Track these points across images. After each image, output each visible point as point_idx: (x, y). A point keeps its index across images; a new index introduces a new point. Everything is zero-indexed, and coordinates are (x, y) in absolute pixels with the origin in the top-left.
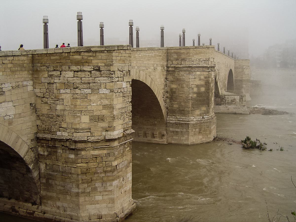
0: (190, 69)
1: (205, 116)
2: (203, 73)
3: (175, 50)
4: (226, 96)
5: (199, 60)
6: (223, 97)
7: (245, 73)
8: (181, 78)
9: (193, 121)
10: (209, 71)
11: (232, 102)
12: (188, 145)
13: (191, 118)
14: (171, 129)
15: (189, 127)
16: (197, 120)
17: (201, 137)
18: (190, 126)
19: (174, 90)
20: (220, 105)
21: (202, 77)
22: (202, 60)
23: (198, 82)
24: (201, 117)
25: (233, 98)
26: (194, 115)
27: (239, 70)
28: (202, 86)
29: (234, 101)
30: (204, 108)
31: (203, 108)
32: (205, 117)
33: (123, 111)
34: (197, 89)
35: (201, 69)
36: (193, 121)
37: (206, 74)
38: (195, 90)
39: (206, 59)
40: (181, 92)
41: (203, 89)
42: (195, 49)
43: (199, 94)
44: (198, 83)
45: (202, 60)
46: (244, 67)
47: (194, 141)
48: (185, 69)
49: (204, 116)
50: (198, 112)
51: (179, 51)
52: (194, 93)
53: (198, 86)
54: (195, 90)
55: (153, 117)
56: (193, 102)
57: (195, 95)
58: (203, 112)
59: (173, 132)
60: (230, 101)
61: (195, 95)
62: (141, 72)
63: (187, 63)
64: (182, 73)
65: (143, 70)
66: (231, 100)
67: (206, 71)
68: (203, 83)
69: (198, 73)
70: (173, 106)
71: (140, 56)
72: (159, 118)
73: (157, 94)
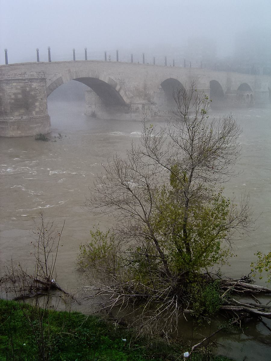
0: (8, 81)
9: (12, 120)
10: (26, 82)
12: (7, 137)
13: (11, 117)
15: (8, 124)
17: (19, 132)
18: (8, 123)
20: (128, 113)
21: (19, 87)
23: (14, 91)
28: (19, 93)
30: (22, 111)
32: (24, 117)
35: (17, 81)
36: (12, 120)
37: (22, 84)
38: (13, 97)
45: (17, 74)
47: (14, 134)
50: (17, 114)
52: (12, 99)
53: (14, 94)
54: (13, 97)
61: (13, 101)
63: (6, 77)
64: (4, 84)
69: (14, 84)
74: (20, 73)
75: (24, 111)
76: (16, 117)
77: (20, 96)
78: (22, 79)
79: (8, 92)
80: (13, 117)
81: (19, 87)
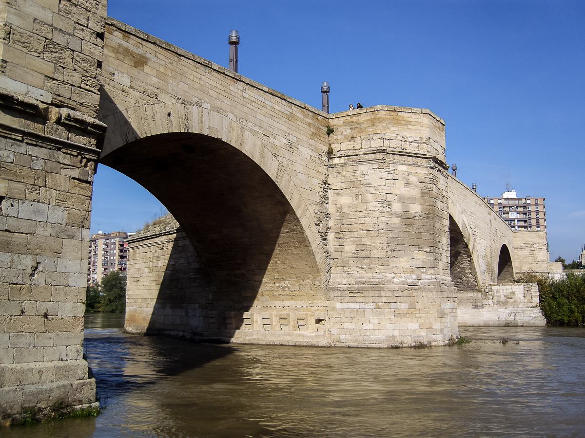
1: (425, 275)
2: (413, 169)
3: (347, 118)
4: (493, 288)
5: (404, 138)
6: (487, 291)
7: (538, 258)
8: (362, 179)
11: (509, 300)
14: (339, 305)
16: (402, 282)
19: (345, 210)
22: (410, 141)
23: (400, 189)
24: (414, 277)
25: (510, 291)
26: (395, 269)
27: (525, 251)
28: (413, 200)
29: (511, 298)
30: (421, 257)
31: (417, 254)
32: (423, 276)
33: (59, 39)
34: (402, 205)
39: (422, 139)
40: (362, 214)
41: (416, 209)
42: (393, 113)
43: (406, 218)
44: (404, 192)
45: (411, 140)
46: (535, 246)
47: (396, 333)
48: (370, 158)
49: (422, 275)
50: (404, 262)
51: (355, 119)
53: (402, 199)
54: (397, 207)
55: (294, 277)
56: (390, 235)
57: (396, 221)
58: (419, 264)
59: (344, 311)
60: (502, 296)
62: (246, 133)
65: (255, 133)
66: (506, 296)
67: (423, 167)
68: (415, 192)
70: (344, 248)
71: (245, 95)
72: (309, 278)
73: (298, 207)
74: (418, 139)
75: (425, 257)
76: (403, 275)
77: (416, 209)
78: (422, 157)
79: (386, 189)
80: (393, 275)
81: (413, 179)
